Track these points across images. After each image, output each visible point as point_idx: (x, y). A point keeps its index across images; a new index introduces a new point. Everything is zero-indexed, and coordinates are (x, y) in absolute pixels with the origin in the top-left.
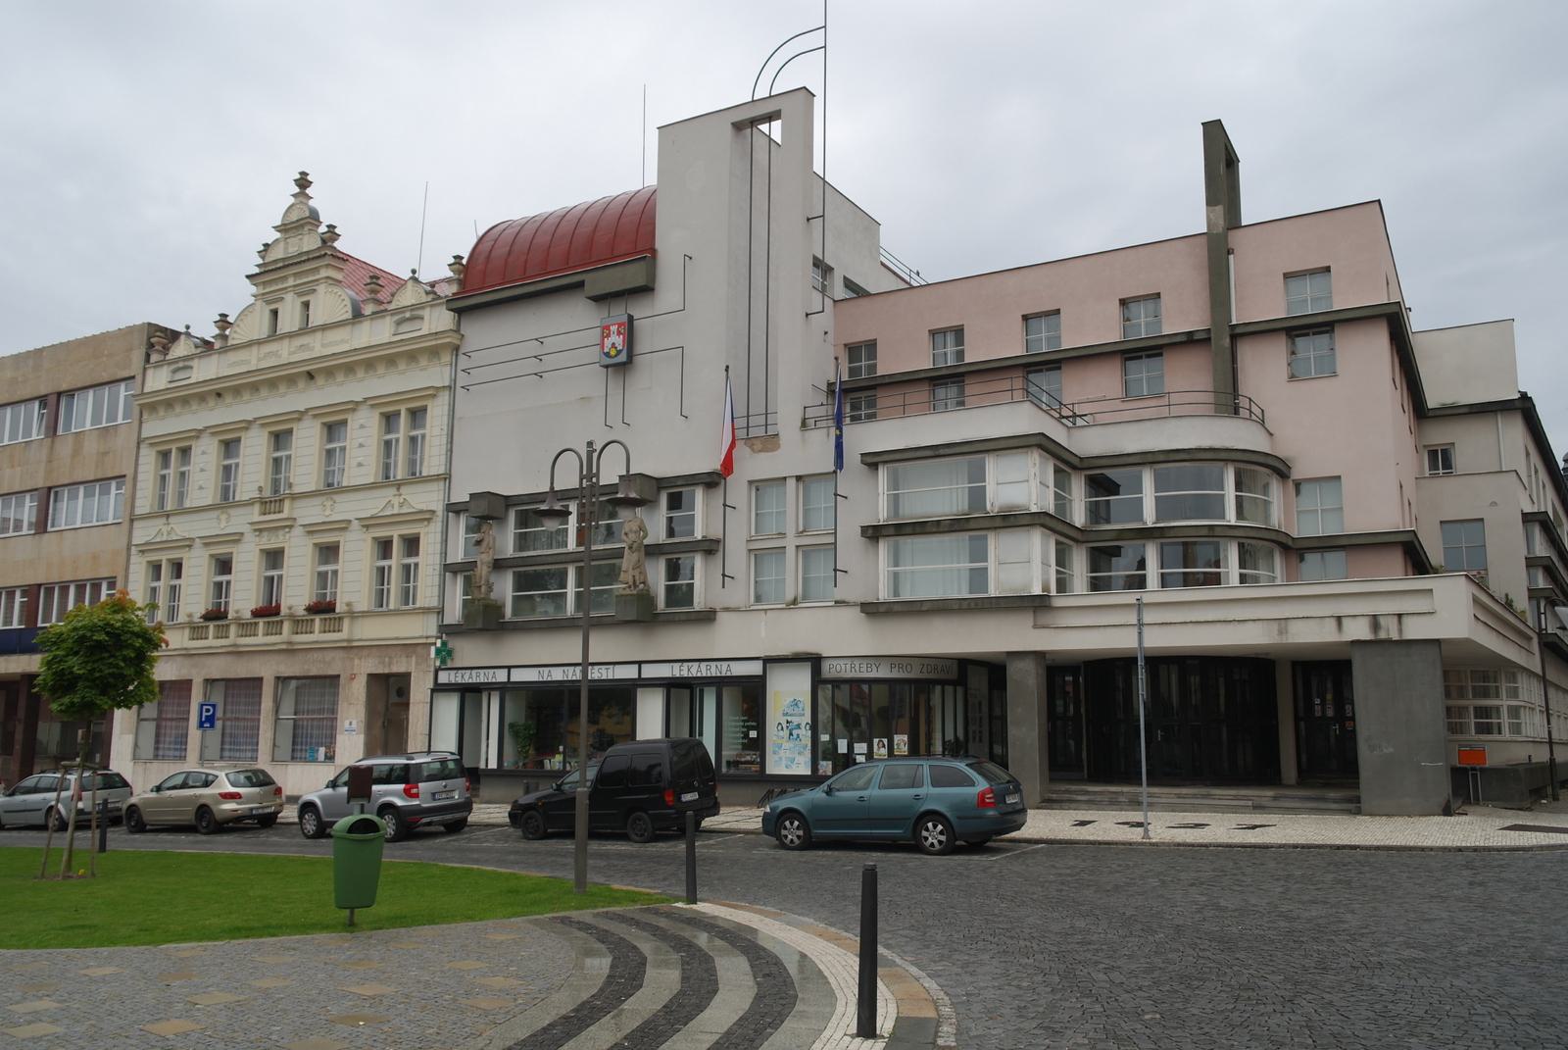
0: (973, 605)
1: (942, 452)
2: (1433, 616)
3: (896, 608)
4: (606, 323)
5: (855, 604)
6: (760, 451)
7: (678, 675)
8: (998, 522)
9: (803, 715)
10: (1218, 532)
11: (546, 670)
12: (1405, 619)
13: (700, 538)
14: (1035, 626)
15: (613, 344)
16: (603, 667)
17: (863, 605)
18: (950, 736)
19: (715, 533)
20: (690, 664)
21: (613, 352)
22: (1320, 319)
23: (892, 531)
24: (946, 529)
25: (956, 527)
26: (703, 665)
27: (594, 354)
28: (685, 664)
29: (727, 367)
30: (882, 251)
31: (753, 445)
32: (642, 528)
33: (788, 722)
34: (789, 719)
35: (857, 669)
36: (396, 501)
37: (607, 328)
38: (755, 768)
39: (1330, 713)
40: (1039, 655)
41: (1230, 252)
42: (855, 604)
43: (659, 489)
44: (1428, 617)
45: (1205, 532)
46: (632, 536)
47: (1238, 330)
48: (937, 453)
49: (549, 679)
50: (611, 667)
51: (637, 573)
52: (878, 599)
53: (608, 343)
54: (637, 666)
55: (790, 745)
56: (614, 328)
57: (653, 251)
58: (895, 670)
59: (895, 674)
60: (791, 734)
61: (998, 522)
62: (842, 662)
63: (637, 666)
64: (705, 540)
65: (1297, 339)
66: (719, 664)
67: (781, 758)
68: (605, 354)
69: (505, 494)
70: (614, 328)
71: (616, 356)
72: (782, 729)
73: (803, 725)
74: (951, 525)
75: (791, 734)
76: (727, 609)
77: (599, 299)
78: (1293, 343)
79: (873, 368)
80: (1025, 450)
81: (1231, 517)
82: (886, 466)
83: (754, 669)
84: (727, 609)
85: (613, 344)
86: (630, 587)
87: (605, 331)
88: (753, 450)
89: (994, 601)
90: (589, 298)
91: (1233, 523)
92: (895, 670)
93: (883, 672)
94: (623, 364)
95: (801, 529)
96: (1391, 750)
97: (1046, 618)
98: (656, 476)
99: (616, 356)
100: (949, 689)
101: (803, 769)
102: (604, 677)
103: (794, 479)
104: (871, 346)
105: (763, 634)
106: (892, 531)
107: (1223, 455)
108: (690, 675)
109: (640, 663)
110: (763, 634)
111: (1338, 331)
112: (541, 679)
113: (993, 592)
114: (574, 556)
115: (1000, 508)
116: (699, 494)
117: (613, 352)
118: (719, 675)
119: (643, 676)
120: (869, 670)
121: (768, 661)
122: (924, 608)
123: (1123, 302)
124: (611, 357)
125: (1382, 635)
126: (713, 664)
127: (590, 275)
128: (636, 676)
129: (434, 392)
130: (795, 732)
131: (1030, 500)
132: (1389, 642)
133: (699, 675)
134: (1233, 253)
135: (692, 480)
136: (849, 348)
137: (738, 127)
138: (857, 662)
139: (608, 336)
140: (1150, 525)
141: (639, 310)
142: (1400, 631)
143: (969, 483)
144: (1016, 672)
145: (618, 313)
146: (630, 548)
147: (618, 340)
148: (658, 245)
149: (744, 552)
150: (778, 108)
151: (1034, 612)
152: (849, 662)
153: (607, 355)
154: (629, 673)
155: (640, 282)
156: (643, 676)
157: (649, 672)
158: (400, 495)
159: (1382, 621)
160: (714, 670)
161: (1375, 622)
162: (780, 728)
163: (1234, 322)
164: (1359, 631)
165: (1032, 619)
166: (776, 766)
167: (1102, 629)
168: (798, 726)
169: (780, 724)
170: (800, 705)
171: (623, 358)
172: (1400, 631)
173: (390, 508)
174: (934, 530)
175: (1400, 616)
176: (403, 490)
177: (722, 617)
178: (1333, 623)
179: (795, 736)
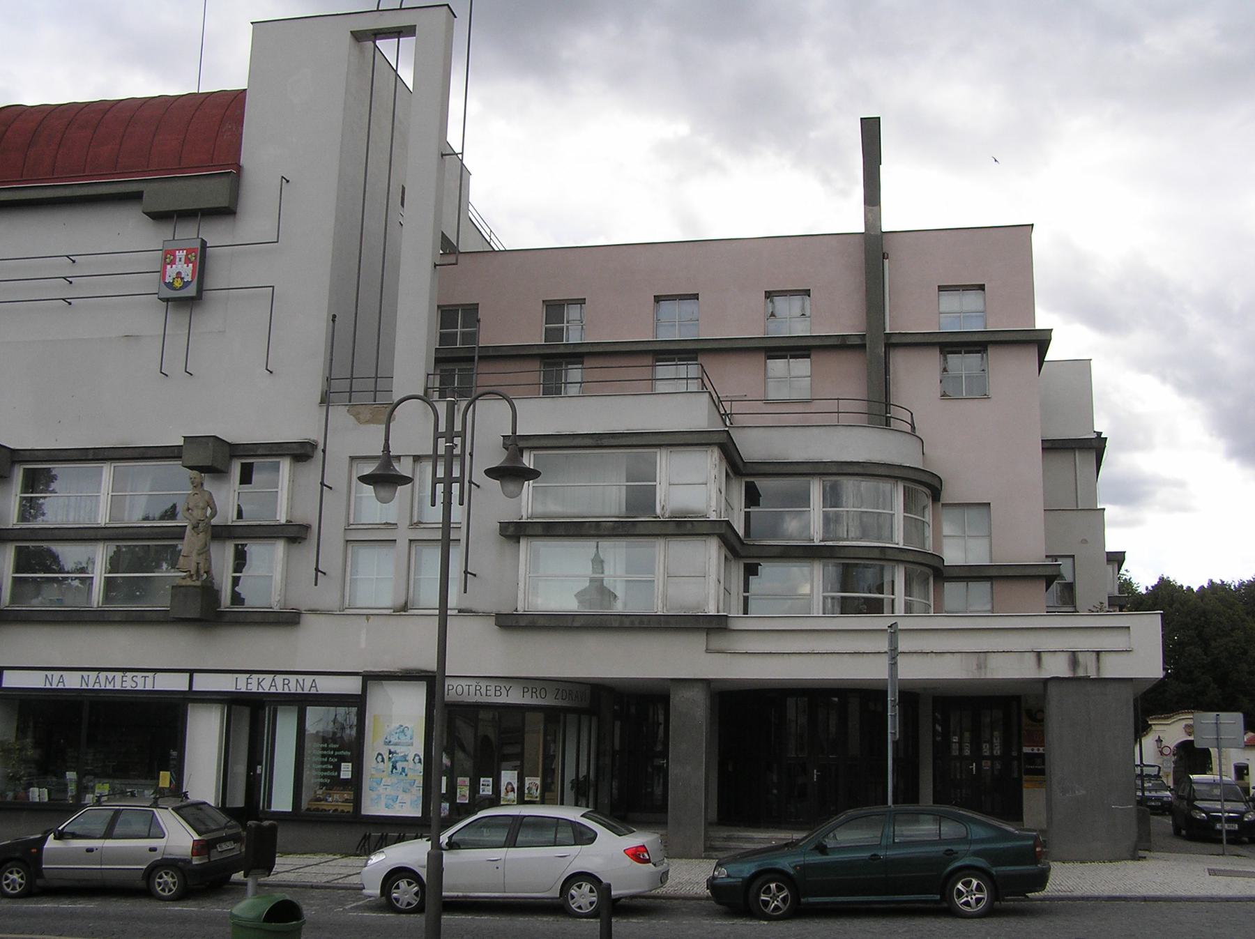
0: (637, 624)
1: (605, 442)
2: (1131, 653)
3: (541, 622)
4: (170, 247)
5: (487, 615)
6: (369, 422)
7: (244, 690)
8: (671, 529)
9: (412, 744)
10: (889, 555)
11: (57, 674)
12: (1103, 656)
13: (283, 521)
14: (708, 651)
15: (179, 273)
16: (140, 674)
17: (498, 616)
18: (583, 771)
19: (306, 514)
20: (261, 676)
21: (178, 284)
22: (975, 338)
23: (539, 531)
24: (606, 533)
25: (620, 531)
26: (279, 678)
27: (151, 283)
28: (255, 676)
29: (334, 316)
30: (470, 208)
31: (359, 413)
32: (210, 503)
33: (390, 753)
34: (393, 748)
35: (484, 693)
37: (173, 253)
38: (349, 808)
39: (967, 752)
40: (707, 682)
41: (885, 256)
42: (487, 615)
43: (233, 456)
44: (1125, 655)
45: (876, 554)
46: (197, 514)
47: (893, 340)
48: (599, 443)
49: (61, 686)
51: (201, 560)
52: (516, 610)
53: (171, 271)
54: (188, 675)
55: (394, 779)
56: (181, 254)
57: (239, 168)
58: (528, 695)
59: (527, 700)
60: (394, 767)
61: (671, 529)
62: (464, 682)
63: (188, 675)
64: (289, 524)
65: (949, 356)
66: (300, 678)
67: (379, 796)
69: (12, 447)
70: (181, 254)
71: (181, 288)
72: (383, 761)
73: (410, 758)
74: (614, 528)
75: (394, 767)
76: (313, 611)
77: (159, 217)
78: (945, 359)
79: (472, 337)
80: (704, 448)
81: (899, 541)
82: (533, 453)
83: (351, 686)
84: (313, 611)
85: (179, 273)
86: (191, 576)
87: (168, 257)
88: (358, 420)
89: (662, 618)
90: (147, 214)
91: (901, 546)
92: (528, 695)
93: (515, 697)
94: (192, 299)
95: (415, 520)
96: (1084, 792)
97: (719, 642)
98: (230, 441)
99: (181, 288)
100: (585, 719)
101: (410, 808)
102: (140, 687)
103: (412, 458)
104: (471, 311)
105: (363, 645)
106: (539, 531)
107: (897, 473)
108: (261, 690)
109: (191, 672)
110: (363, 645)
111: (992, 352)
112: (48, 686)
114: (106, 532)
115: (672, 513)
116: (285, 465)
117: (178, 284)
118: (300, 691)
119: (194, 689)
120: (498, 693)
121: (369, 678)
122: (576, 624)
123: (769, 295)
124: (175, 289)
125: (1081, 673)
126: (293, 678)
127: (155, 186)
128: (187, 689)
130: (399, 765)
131: (709, 506)
132: (1087, 679)
133: (273, 690)
134: (887, 258)
135: (276, 450)
136: (442, 311)
137: (358, 36)
138: (483, 684)
139: (173, 262)
140: (817, 543)
141: (215, 234)
142: (1098, 669)
143: (627, 482)
144: (679, 699)
145: (188, 233)
146: (195, 527)
147: (187, 271)
148: (243, 162)
149: (342, 543)
150: (412, 23)
151: (707, 634)
152: (473, 683)
153: (170, 286)
154: (178, 683)
155: (222, 202)
156: (194, 689)
157: (204, 683)
159: (1081, 657)
160: (293, 685)
161: (1074, 659)
162: (380, 758)
163: (887, 331)
164: (1057, 667)
165: (705, 637)
166: (375, 805)
167: (786, 656)
168: (405, 759)
169: (379, 754)
170: (409, 733)
171: (191, 291)
172: (1098, 669)
174: (592, 532)
175: (1098, 653)
177: (307, 619)
178: (1032, 658)
179: (399, 769)
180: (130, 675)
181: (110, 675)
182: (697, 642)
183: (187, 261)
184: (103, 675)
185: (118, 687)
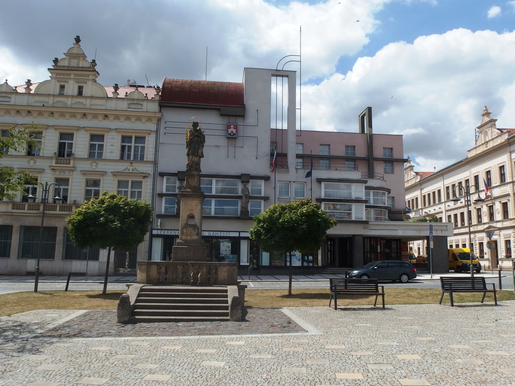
4: (229, 124)
16: (225, 232)
36: (131, 168)
50: (228, 232)
54: (238, 233)
56: (232, 126)
57: (244, 105)
63: (238, 233)
68: (229, 134)
70: (232, 126)
71: (233, 135)
85: (232, 132)
99: (233, 135)
109: (239, 232)
113: (353, 219)
117: (232, 134)
128: (238, 236)
129: (149, 132)
139: (230, 128)
141: (240, 122)
145: (232, 120)
153: (230, 134)
154: (236, 235)
157: (243, 235)
158: (133, 166)
173: (127, 170)
176: (134, 164)
180: (222, 232)
181: (217, 232)
182: (361, 226)
183: (234, 128)
184: (215, 232)
185: (219, 235)
